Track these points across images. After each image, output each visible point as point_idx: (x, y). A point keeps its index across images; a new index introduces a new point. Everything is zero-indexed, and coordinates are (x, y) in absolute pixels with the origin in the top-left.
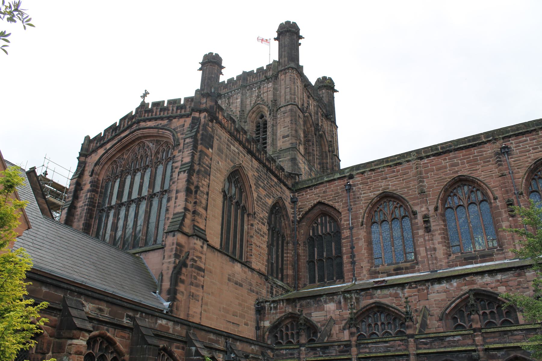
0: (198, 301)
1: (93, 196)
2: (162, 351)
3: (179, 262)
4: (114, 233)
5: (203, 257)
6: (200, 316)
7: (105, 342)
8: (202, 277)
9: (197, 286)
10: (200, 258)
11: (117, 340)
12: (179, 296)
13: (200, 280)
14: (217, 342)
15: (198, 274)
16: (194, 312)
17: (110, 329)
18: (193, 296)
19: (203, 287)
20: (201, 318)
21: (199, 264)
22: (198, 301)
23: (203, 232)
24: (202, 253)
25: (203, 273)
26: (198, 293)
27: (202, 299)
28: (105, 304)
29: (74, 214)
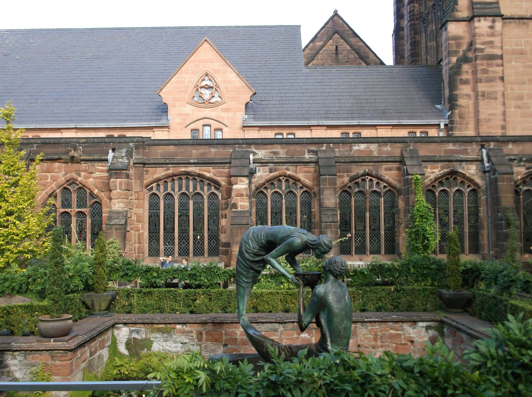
0: (496, 99)
1: (412, 9)
2: (367, 177)
3: (457, 61)
4: (434, 42)
5: (497, 40)
6: (502, 117)
7: (290, 180)
8: (498, 66)
9: (490, 80)
10: (491, 42)
11: (301, 176)
12: (461, 102)
13: (493, 72)
14: (465, 152)
15: (488, 65)
16: (490, 114)
17: (290, 168)
18: (483, 96)
19: (502, 79)
20: (504, 120)
21: (489, 51)
22: (496, 99)
23: (493, 6)
24: (493, 35)
25: (500, 61)
26: (493, 90)
27: (503, 95)
28: (279, 146)
29: (403, 36)
